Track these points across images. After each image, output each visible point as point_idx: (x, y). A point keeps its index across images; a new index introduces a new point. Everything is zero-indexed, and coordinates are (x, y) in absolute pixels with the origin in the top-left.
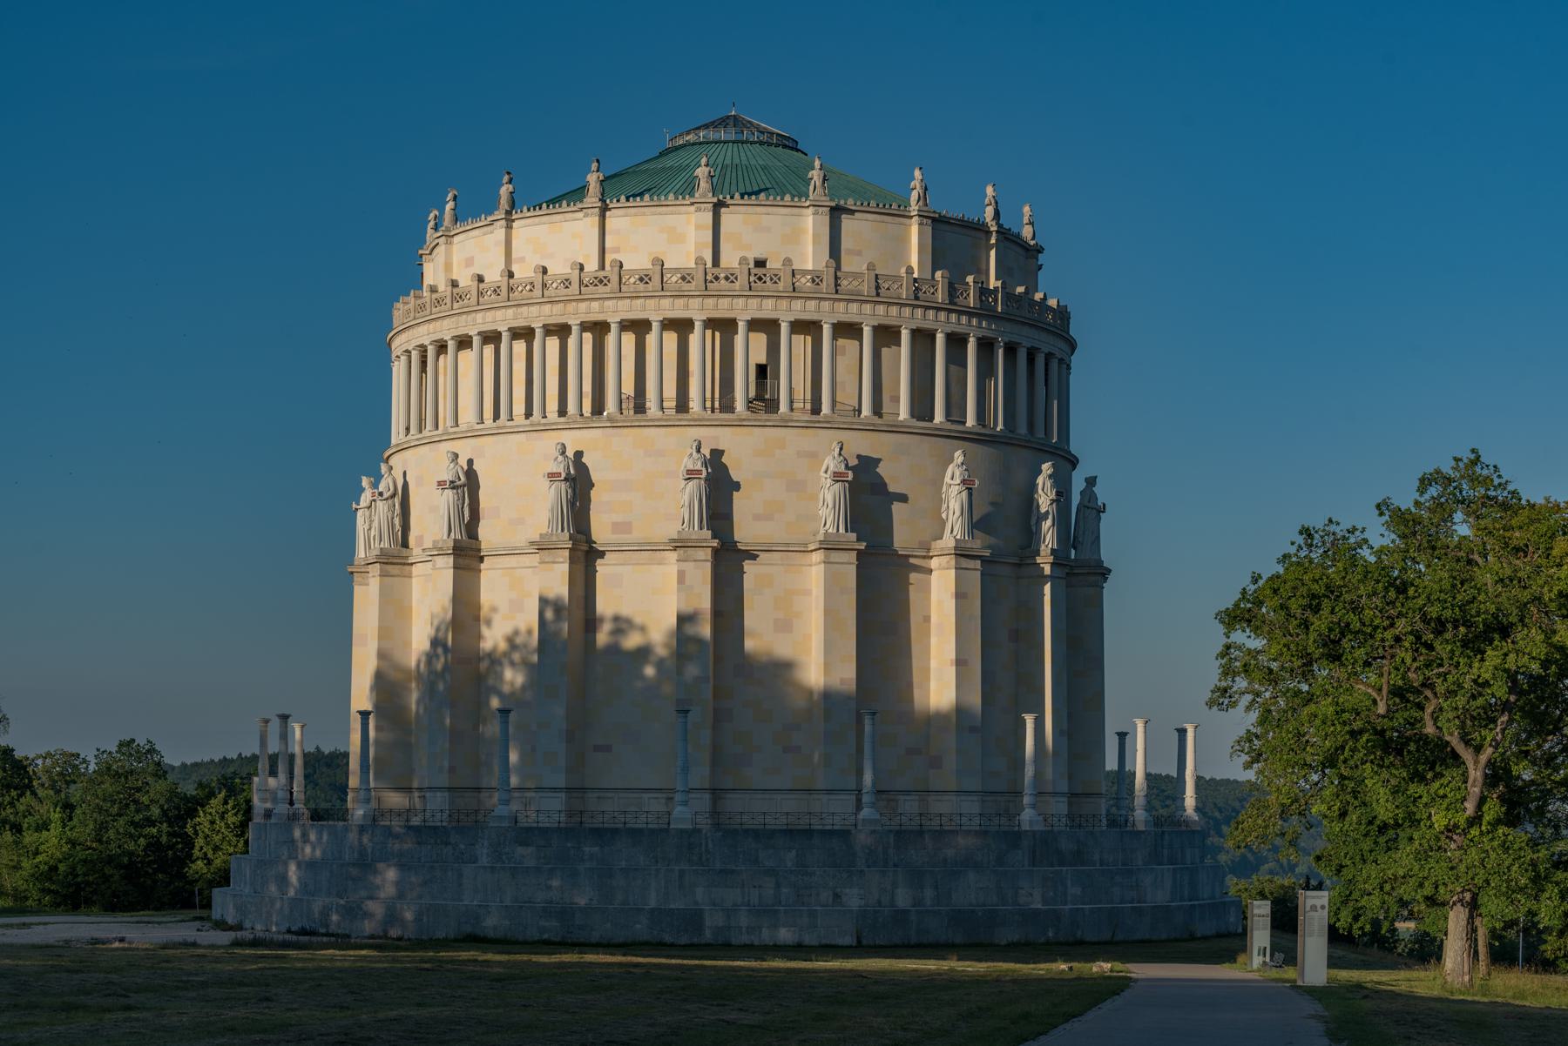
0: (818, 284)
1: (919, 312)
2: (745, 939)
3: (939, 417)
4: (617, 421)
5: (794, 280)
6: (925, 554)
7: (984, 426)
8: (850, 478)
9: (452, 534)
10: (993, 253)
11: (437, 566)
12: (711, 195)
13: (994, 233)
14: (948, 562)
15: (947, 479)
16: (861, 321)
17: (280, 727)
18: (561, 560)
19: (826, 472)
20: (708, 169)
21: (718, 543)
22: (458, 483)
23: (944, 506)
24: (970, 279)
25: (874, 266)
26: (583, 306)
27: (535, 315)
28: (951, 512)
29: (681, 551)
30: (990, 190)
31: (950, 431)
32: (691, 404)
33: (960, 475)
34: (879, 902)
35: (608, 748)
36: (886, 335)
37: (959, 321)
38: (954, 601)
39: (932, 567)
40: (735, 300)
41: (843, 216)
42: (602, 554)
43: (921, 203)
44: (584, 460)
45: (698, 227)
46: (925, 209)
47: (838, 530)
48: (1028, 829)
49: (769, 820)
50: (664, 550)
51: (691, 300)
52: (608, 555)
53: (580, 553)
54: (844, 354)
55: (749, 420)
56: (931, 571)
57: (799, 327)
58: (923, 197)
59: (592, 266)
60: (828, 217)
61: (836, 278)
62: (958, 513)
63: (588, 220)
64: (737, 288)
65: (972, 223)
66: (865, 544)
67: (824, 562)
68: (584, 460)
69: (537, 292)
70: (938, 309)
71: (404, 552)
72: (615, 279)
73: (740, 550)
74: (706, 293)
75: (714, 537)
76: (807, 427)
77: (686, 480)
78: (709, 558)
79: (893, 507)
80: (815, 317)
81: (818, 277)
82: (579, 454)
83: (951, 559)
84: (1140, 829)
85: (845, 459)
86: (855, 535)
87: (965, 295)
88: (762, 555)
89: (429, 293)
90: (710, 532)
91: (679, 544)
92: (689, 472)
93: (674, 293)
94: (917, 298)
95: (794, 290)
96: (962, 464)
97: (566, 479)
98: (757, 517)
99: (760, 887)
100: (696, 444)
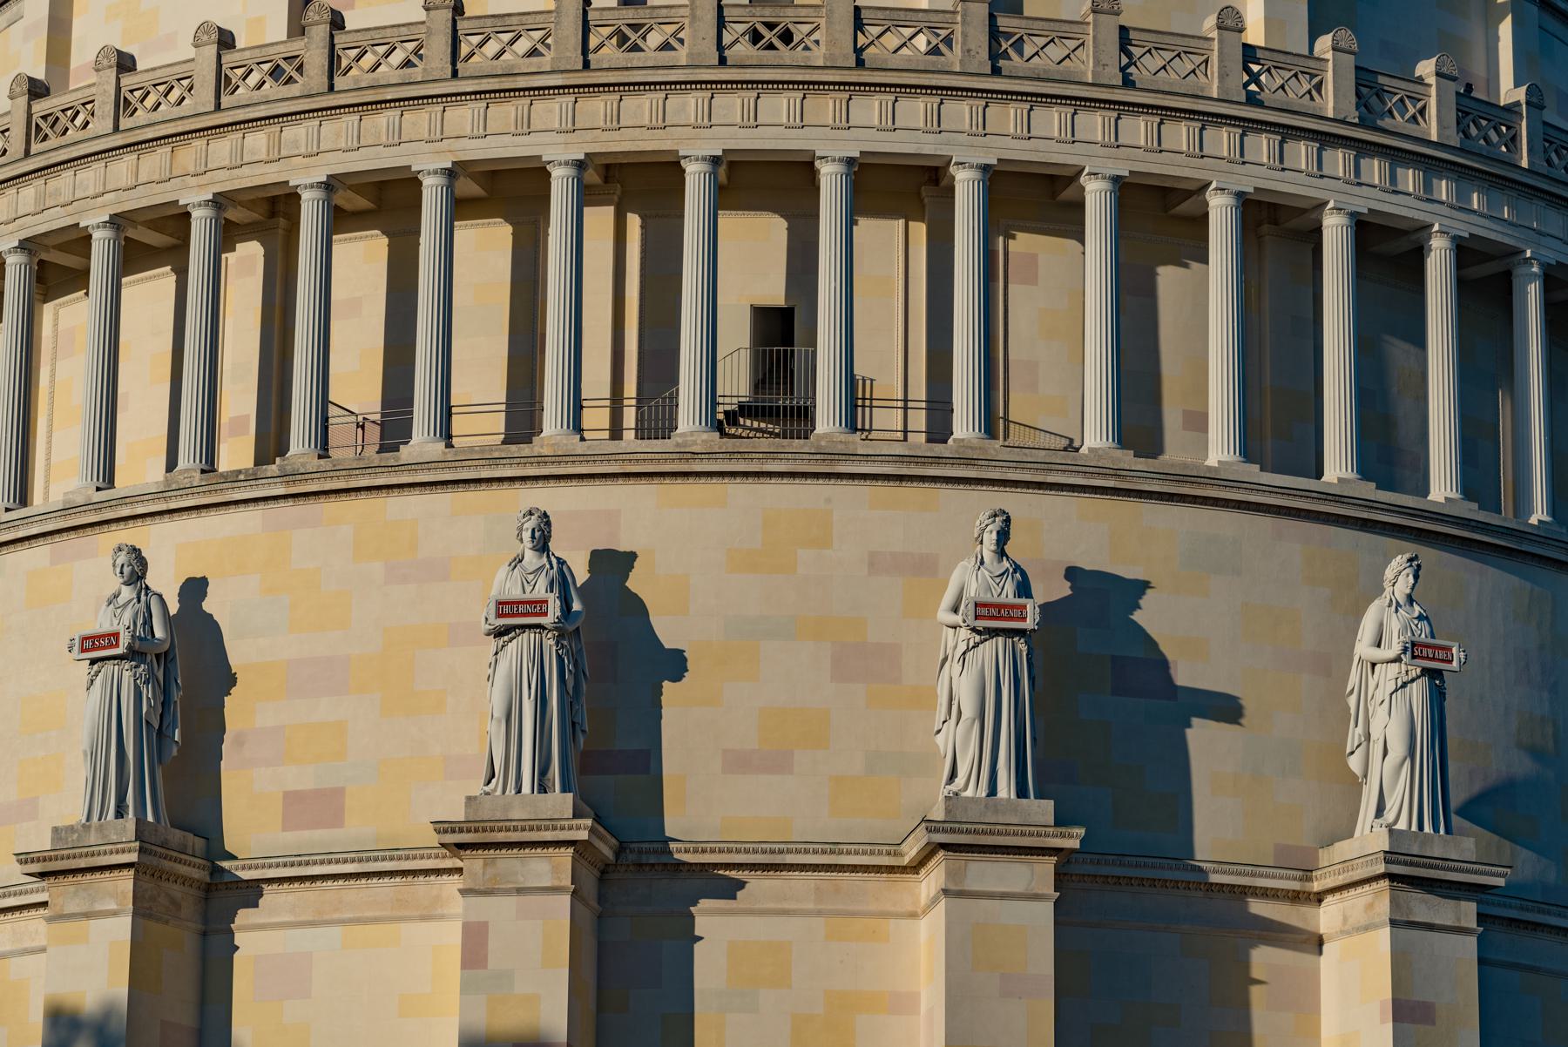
1: (1262, 146)
3: (1337, 466)
5: (862, 40)
6: (1295, 885)
10: (1506, 29)
14: (1370, 906)
15: (1363, 648)
18: (113, 906)
19: (955, 610)
21: (592, 831)
23: (1355, 734)
24: (1426, 68)
26: (222, 148)
27: (91, 192)
28: (1377, 750)
29: (473, 863)
31: (1370, 505)
33: (1405, 628)
37: (1393, 178)
38: (1390, 1025)
39: (1321, 932)
42: (251, 893)
44: (208, 606)
47: (993, 791)
50: (438, 872)
52: (270, 896)
53: (176, 890)
54: (1031, 279)
55: (710, 455)
56: (1320, 942)
61: (994, 34)
62: (1397, 749)
66: (1081, 831)
67: (946, 892)
68: (208, 606)
69: (101, 124)
70: (1325, 140)
72: (316, 60)
73: (681, 865)
75: (576, 815)
76: (900, 478)
77: (499, 633)
78: (566, 881)
79: (1189, 732)
80: (927, 146)
82: (195, 589)
83: (1377, 894)
85: (1017, 568)
86: (1049, 805)
87: (1412, 110)
92: (505, 607)
95: (860, 63)
96: (1410, 600)
97: (133, 654)
98: (739, 763)
100: (532, 523)
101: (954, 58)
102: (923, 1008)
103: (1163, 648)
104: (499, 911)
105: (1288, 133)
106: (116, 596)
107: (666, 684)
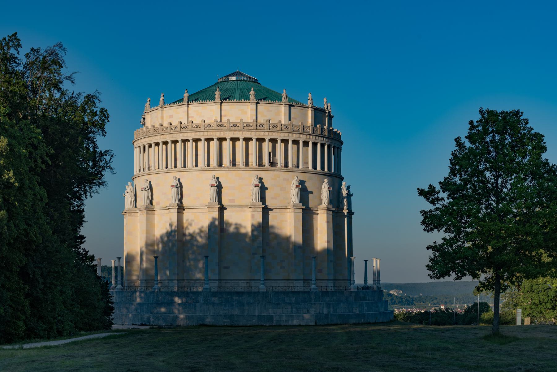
0: (288, 128)
2: (285, 324)
4: (230, 169)
7: (329, 171)
8: (300, 187)
9: (176, 202)
10: (327, 118)
11: (171, 212)
12: (255, 100)
13: (327, 113)
14: (324, 212)
15: (323, 187)
16: (299, 140)
17: (118, 261)
18: (216, 211)
19: (293, 185)
20: (254, 92)
22: (178, 186)
23: (322, 195)
25: (303, 123)
26: (218, 133)
28: (324, 197)
30: (325, 100)
31: (322, 173)
32: (250, 164)
33: (327, 186)
34: (320, 312)
35: (228, 268)
36: (306, 144)
38: (326, 224)
40: (265, 133)
41: (292, 107)
42: (226, 209)
43: (311, 104)
45: (251, 110)
46: (312, 106)
48: (353, 290)
49: (287, 289)
51: (252, 132)
52: (227, 209)
57: (283, 141)
58: (312, 102)
59: (219, 120)
60: (288, 108)
62: (327, 197)
63: (217, 106)
64: (266, 129)
65: (322, 110)
67: (294, 212)
70: (319, 136)
71: (152, 207)
74: (257, 130)
81: (288, 126)
84: (375, 290)
88: (274, 209)
89: (160, 126)
90: (262, 203)
91: (253, 206)
92: (256, 185)
93: (247, 130)
94: (314, 133)
99: (287, 308)
100: (257, 176)
101: (290, 128)
102: (288, 221)
103: (307, 187)
104: (255, 213)
105: (316, 136)
106: (212, 179)
107: (266, 191)
